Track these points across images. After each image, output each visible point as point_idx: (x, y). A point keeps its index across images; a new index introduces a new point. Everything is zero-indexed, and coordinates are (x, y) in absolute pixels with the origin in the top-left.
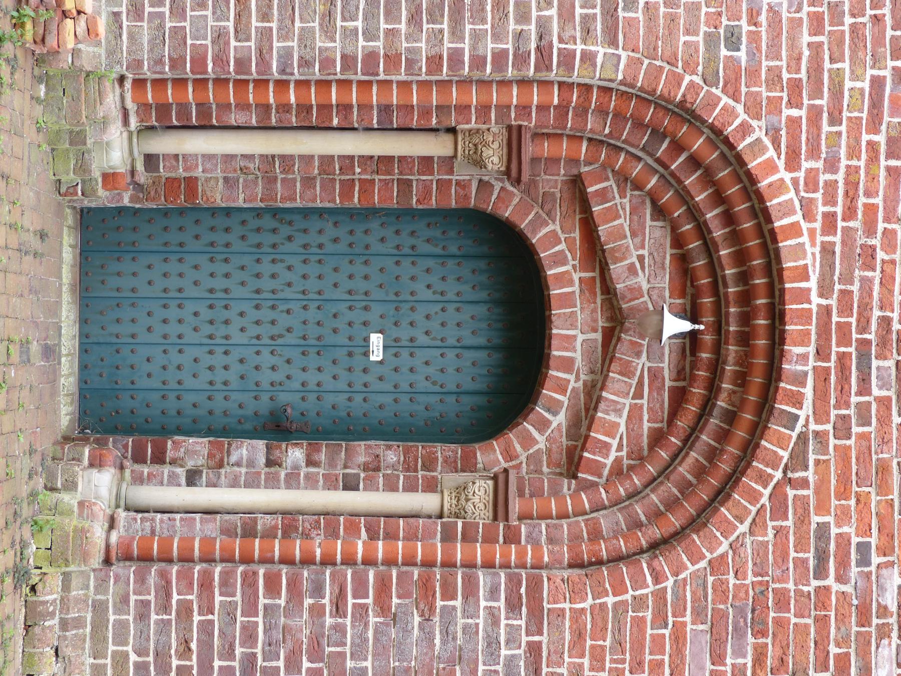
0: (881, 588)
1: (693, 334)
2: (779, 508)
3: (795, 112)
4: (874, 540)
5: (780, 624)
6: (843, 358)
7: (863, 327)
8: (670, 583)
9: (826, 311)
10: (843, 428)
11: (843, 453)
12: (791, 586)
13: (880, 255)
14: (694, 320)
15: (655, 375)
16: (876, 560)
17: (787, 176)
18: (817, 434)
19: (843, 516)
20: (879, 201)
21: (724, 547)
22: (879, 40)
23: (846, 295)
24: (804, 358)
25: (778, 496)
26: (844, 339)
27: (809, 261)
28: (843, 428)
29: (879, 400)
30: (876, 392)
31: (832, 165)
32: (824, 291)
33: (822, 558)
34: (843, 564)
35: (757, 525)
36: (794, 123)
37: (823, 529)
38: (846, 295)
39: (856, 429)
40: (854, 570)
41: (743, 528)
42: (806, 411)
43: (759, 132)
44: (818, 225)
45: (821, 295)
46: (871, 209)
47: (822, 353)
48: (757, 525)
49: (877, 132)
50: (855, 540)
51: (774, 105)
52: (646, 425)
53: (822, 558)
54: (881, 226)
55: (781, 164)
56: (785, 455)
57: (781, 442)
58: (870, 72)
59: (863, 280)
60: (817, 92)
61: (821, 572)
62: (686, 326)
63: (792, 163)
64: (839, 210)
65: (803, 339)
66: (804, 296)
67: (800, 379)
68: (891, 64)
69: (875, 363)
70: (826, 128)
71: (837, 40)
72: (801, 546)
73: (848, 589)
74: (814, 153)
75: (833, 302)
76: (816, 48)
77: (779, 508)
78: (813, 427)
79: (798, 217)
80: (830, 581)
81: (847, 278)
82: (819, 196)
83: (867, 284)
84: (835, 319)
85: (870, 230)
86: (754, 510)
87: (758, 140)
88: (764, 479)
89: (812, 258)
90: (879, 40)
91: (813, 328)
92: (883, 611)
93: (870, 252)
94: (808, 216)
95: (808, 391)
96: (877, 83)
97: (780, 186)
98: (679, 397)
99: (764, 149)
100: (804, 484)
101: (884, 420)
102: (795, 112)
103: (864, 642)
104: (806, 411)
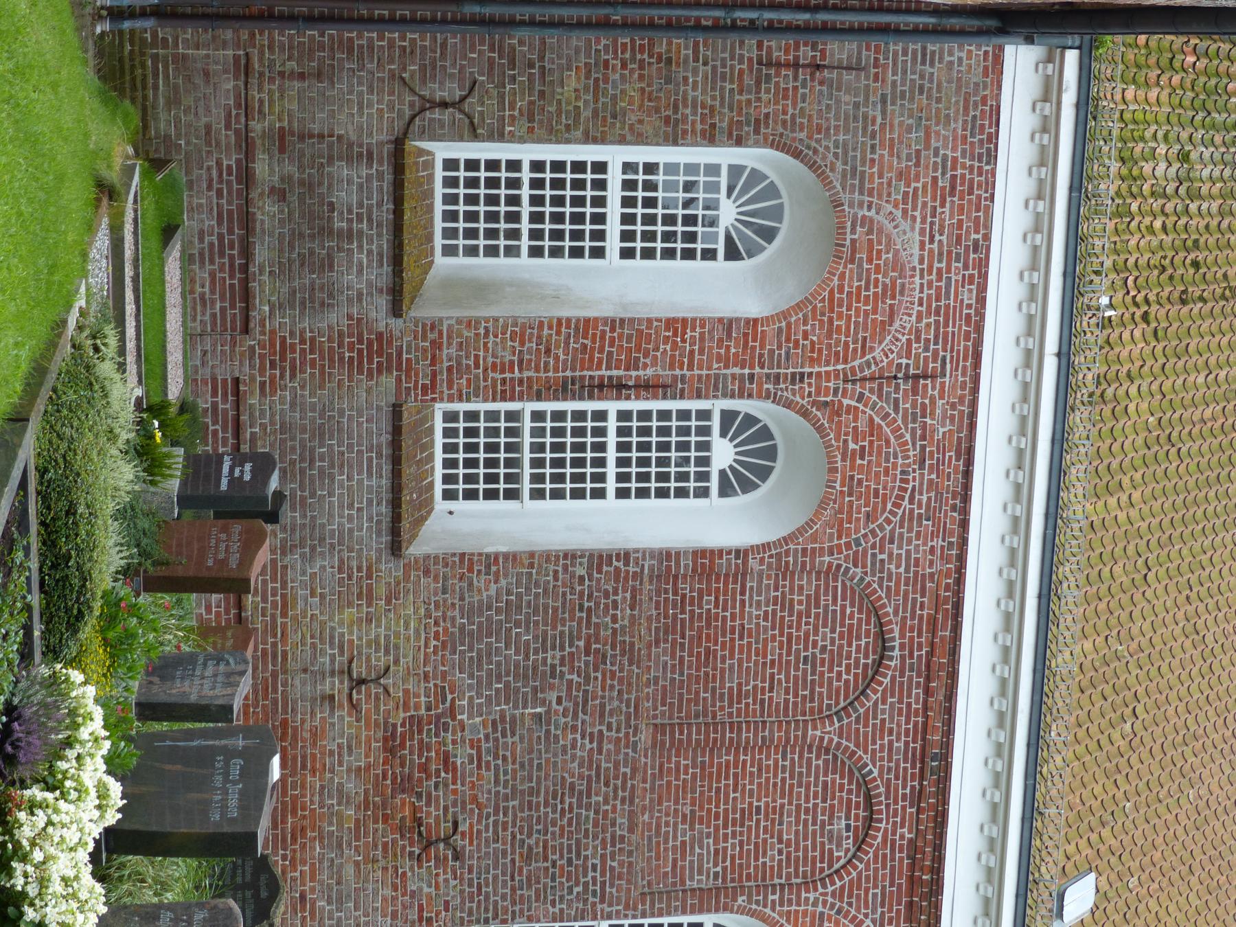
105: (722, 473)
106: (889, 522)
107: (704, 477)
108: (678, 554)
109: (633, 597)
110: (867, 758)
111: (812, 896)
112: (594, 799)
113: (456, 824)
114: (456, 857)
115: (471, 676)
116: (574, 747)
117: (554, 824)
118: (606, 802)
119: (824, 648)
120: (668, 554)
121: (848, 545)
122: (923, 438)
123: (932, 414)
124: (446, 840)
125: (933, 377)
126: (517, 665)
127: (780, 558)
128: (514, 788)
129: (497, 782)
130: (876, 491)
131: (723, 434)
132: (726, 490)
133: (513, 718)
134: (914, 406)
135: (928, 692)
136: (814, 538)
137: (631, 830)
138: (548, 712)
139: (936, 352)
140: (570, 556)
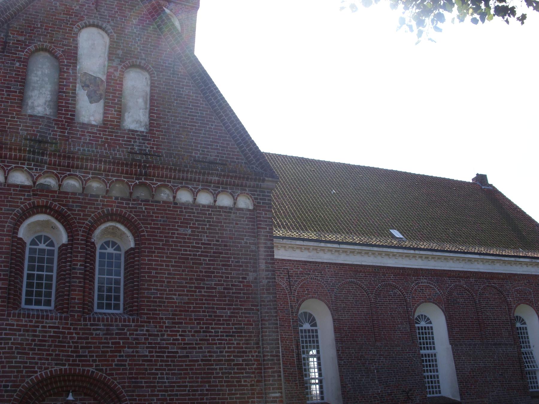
0: (128, 352)
1: (72, 392)
2: (112, 374)
3: (24, 372)
4: (118, 354)
5: (136, 374)
6: (80, 361)
7: (73, 356)
8: (127, 398)
9: (69, 365)
10: (94, 361)
11: (99, 361)
12: (128, 372)
13: (57, 353)
14: (69, 392)
15: (81, 400)
16: (122, 354)
17: (39, 373)
18: (96, 366)
19: (113, 361)
20: (45, 353)
21: (119, 386)
22: (8, 353)
23: (66, 360)
24: (80, 369)
25: (109, 375)
26: (75, 361)
27: (58, 368)
28: (94, 361)
29: (89, 353)
30: (87, 354)
31: (37, 363)
32: (65, 365)
33: (122, 365)
34: (123, 361)
35: (115, 379)
36: (27, 372)
37: (116, 365)
38: (66, 360)
39: (95, 358)
40: (124, 358)
41: (115, 382)
42: (91, 369)
43: (28, 380)
44: (50, 367)
45: (65, 366)
46: (47, 355)
47: (78, 365)
48: (115, 379)
49: (29, 353)
50: (118, 358)
51: (22, 376)
52: (92, 402)
53: (122, 365)
54: (51, 352)
55: (36, 375)
56: (100, 373)
57: (97, 374)
58: (16, 355)
59: (62, 356)
60: (20, 367)
61: (125, 365)
62: (71, 394)
63: (36, 372)
64: (47, 362)
65: (75, 369)
66: (66, 369)
67: (84, 370)
68: (14, 350)
69: (81, 354)
70: (28, 365)
71: (8, 362)
72: (119, 369)
73: (128, 359)
74: (34, 367)
75: (67, 363)
76: (9, 367)
77: (112, 374)
78: (94, 367)
79: (48, 371)
80: (127, 363)
81: (62, 360)
82: (43, 366)
83: (63, 356)
84: (71, 363)
85: (51, 355)
86: (112, 380)
87: (30, 380)
88: (105, 378)
89: (58, 368)
90: (8, 353)
91: (73, 367)
92: (133, 352)
93: (56, 355)
94: (48, 368)
95: (86, 368)
96: (18, 353)
97: (41, 375)
98: (86, 394)
99: (32, 379)
100: (106, 369)
101: (93, 352)
102: (24, 372)
103: (139, 356)
104: (91, 369)
105: (311, 326)
106: (323, 283)
107: (312, 330)
108: (336, 337)
109: (347, 348)
110: (377, 287)
111: (408, 300)
112: (394, 356)
113: (403, 391)
114: (411, 391)
115: (370, 390)
116: (382, 362)
117: (400, 366)
118: (394, 353)
119: (353, 298)
120: (336, 340)
121: (330, 293)
122: (303, 274)
123: (297, 272)
124: (407, 393)
125: (288, 271)
126: (366, 378)
127: (334, 311)
128: (394, 377)
129: (393, 381)
130: (317, 286)
131: (302, 326)
132: (315, 325)
133: (379, 378)
134: (295, 276)
135: (361, 271)
136: (329, 302)
137: (400, 346)
138: (376, 369)
139: (283, 271)
140: (339, 365)
